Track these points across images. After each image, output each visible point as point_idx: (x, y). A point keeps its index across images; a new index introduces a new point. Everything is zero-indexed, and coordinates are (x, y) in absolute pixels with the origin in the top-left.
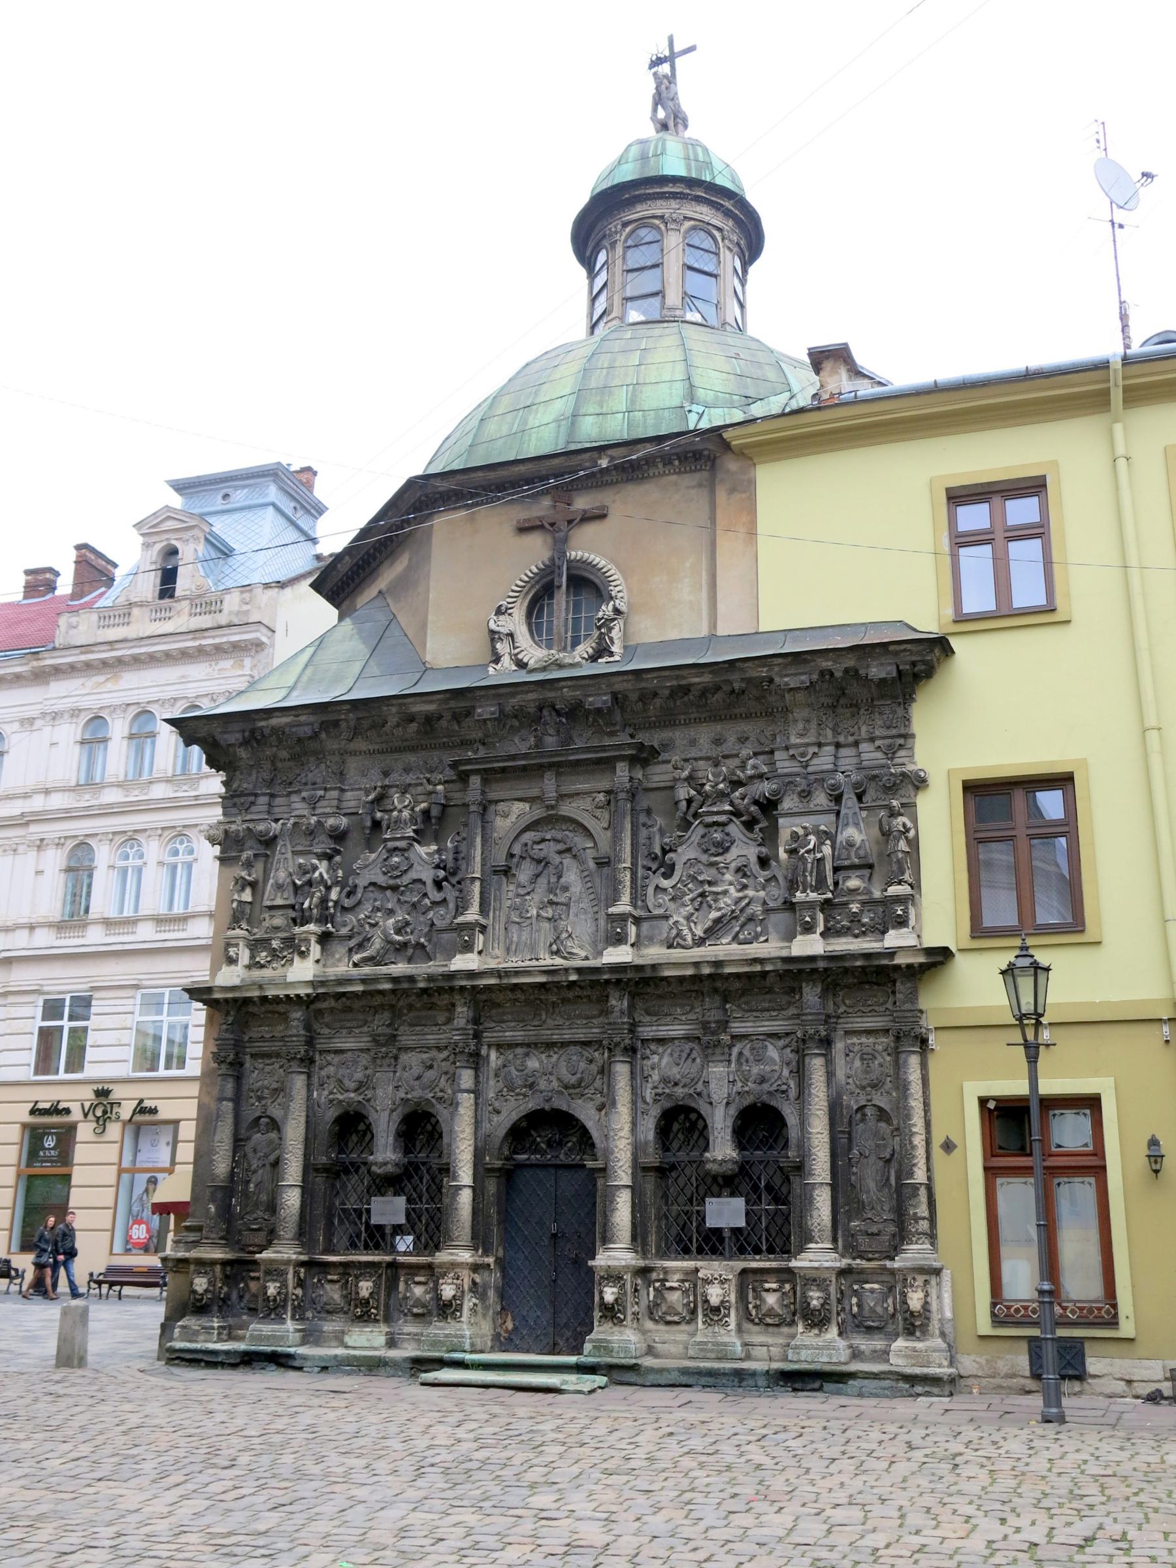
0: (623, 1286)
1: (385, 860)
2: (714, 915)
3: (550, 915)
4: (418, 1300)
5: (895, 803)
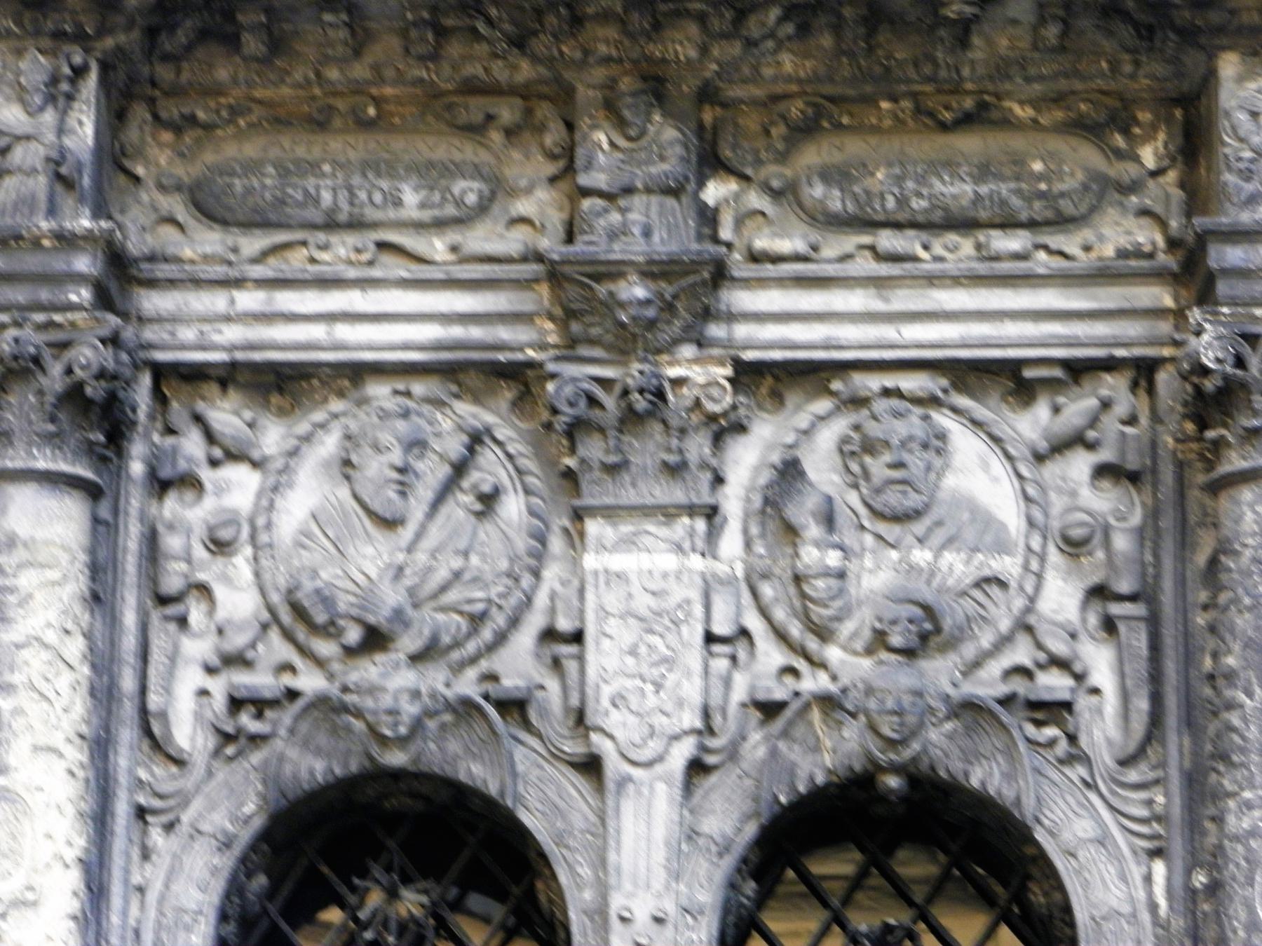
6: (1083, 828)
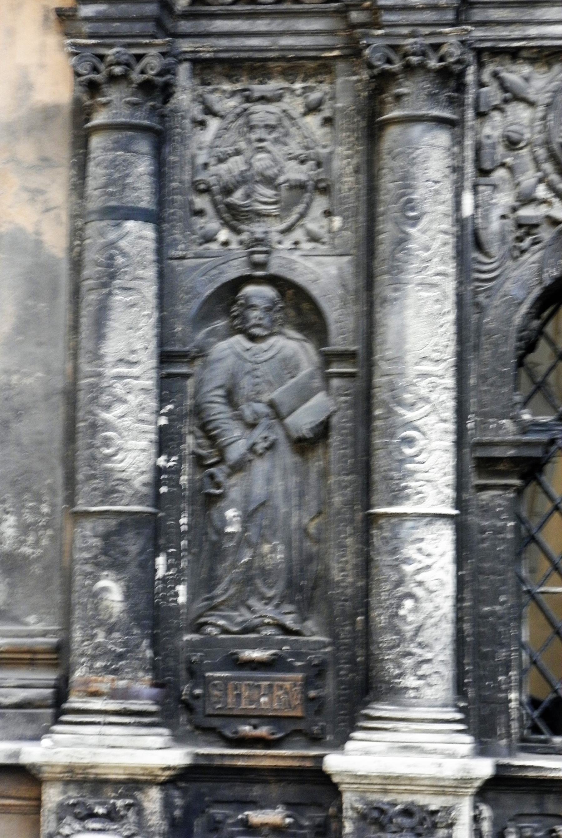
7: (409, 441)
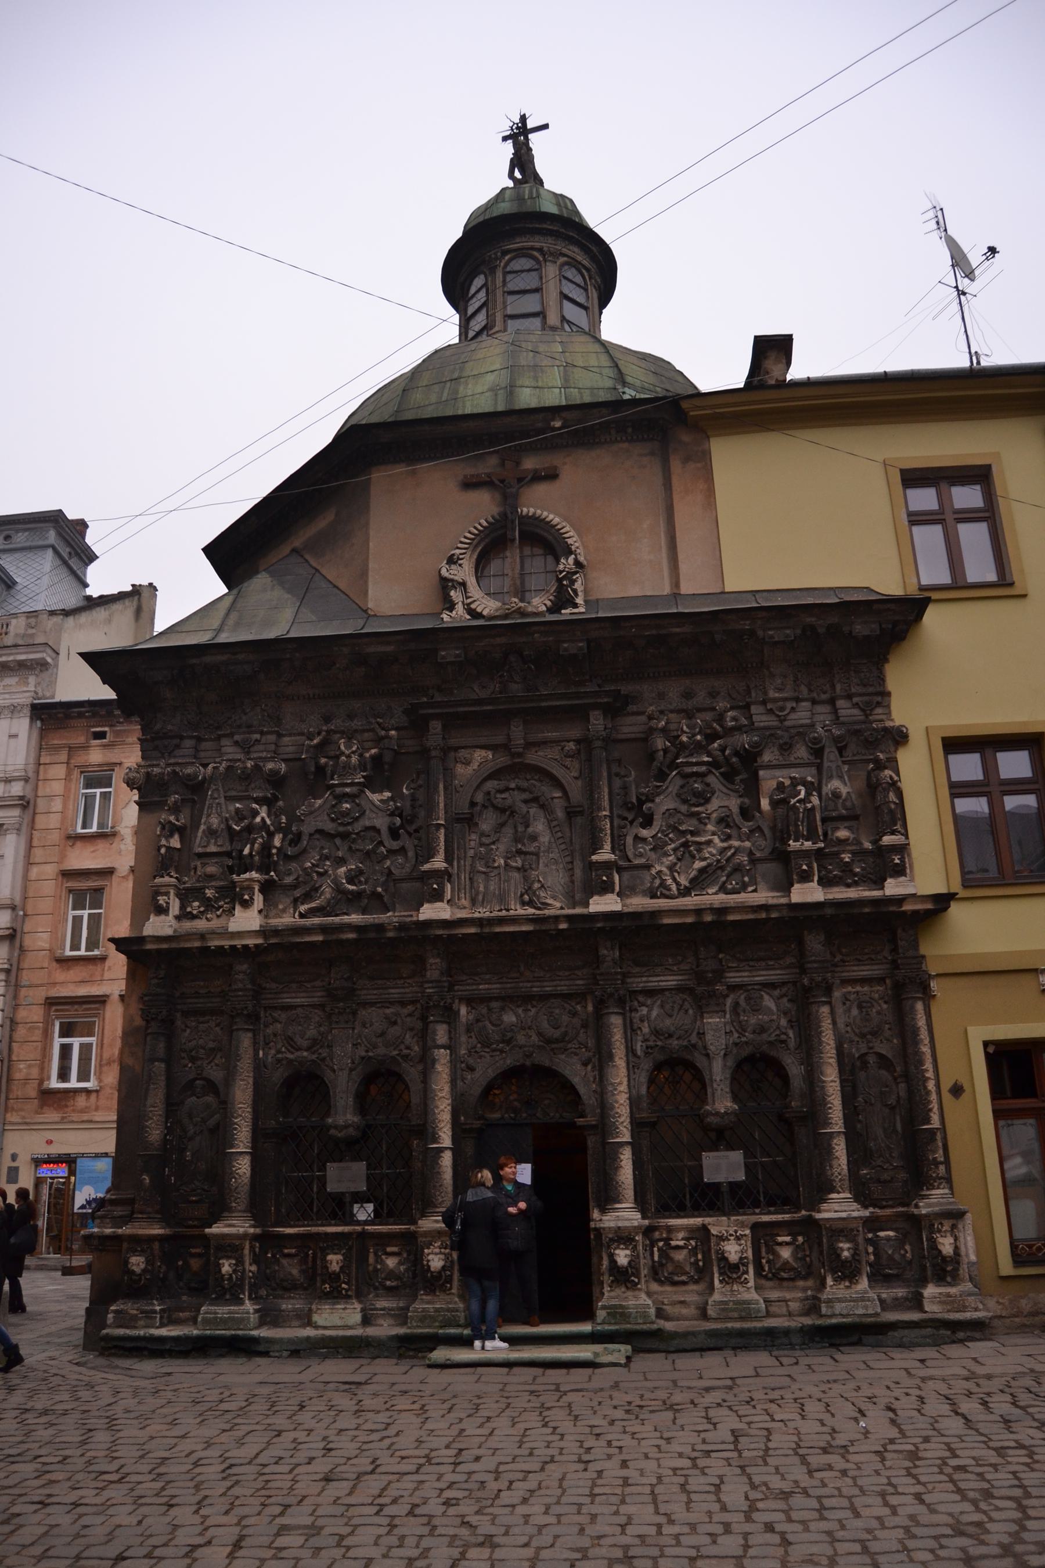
0: (635, 1248)
1: (334, 806)
2: (698, 865)
3: (519, 864)
4: (392, 1271)
5: (881, 756)
6: (790, 1061)
7: (236, 1129)
